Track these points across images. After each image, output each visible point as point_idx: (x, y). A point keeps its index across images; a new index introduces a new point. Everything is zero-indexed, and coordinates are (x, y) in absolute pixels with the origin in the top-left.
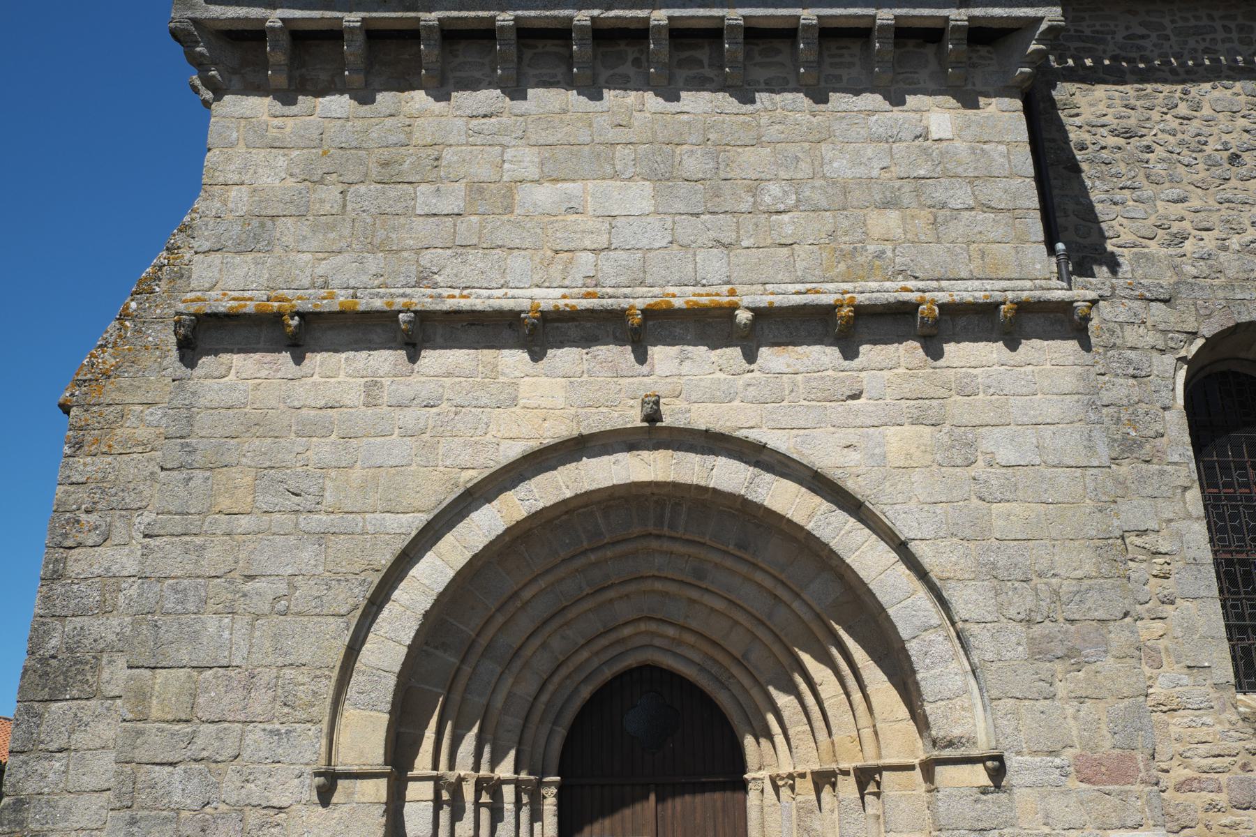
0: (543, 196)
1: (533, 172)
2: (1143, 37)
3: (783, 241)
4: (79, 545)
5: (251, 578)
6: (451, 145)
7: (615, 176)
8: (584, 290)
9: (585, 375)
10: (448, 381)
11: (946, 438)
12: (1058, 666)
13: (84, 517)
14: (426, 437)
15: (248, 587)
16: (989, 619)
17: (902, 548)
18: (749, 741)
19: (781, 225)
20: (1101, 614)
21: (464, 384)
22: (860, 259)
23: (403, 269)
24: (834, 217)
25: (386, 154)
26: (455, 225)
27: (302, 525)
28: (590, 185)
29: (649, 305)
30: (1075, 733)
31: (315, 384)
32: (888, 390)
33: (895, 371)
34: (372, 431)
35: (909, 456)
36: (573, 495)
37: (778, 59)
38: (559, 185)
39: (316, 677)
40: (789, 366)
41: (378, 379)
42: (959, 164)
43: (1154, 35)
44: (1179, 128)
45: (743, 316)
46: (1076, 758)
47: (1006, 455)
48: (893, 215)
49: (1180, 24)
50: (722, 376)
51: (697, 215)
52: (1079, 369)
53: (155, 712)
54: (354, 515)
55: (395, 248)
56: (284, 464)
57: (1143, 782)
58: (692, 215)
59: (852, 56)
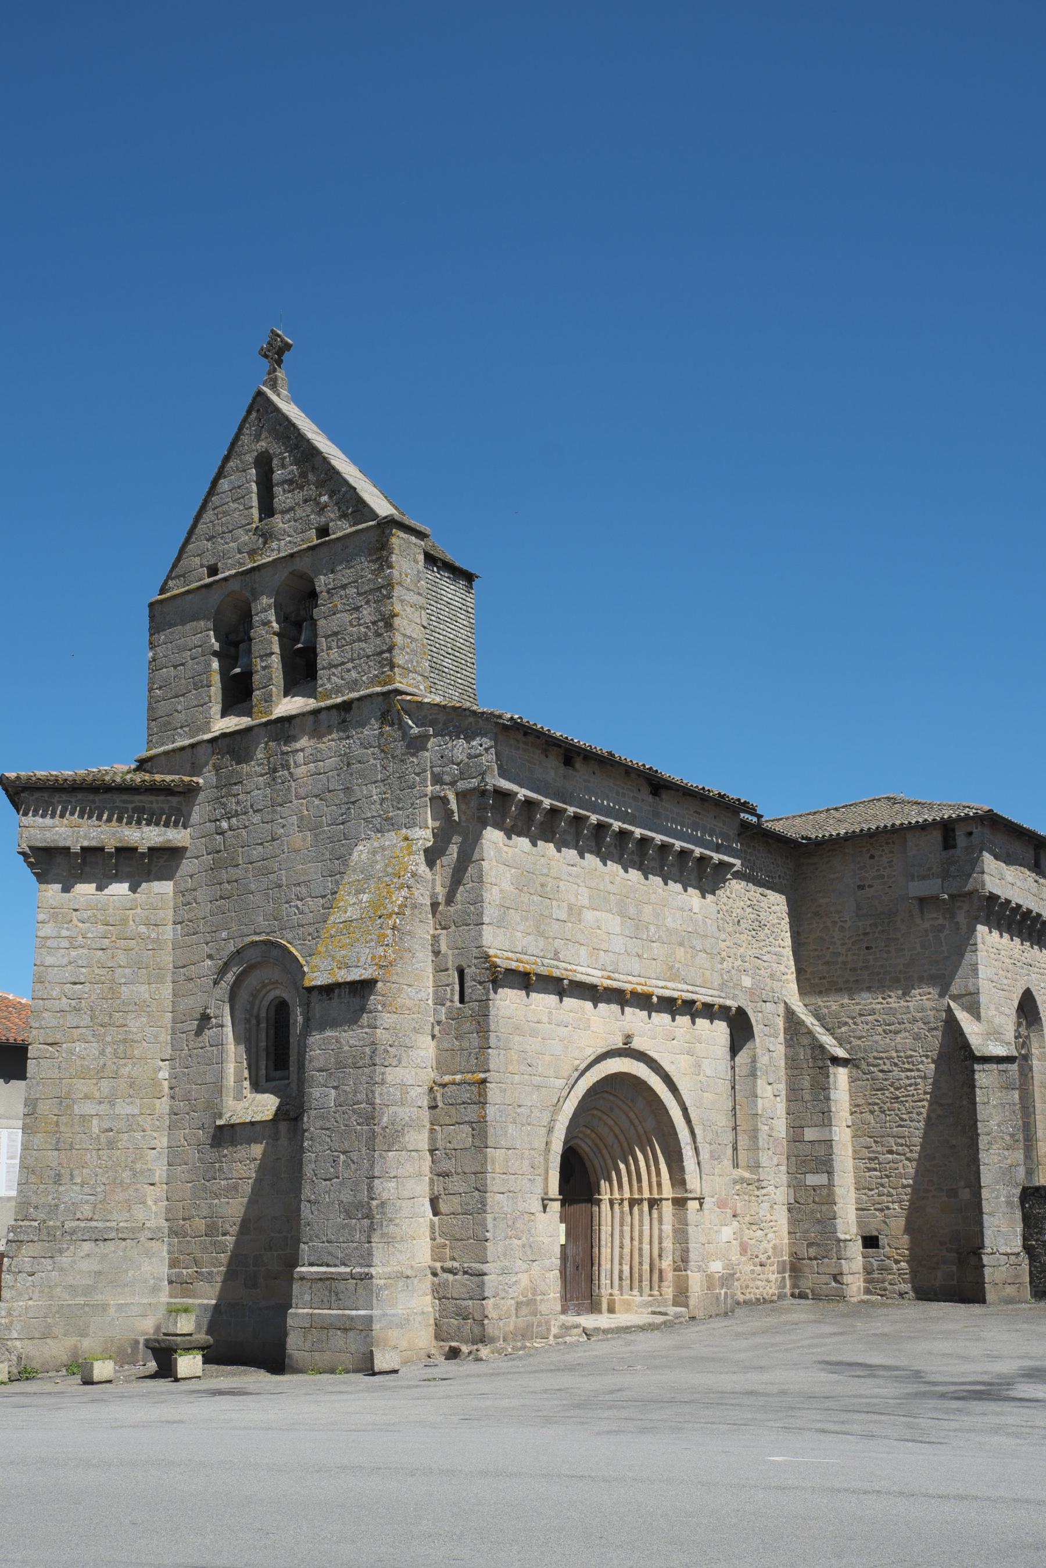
1: (586, 902)
5: (519, 1106)
8: (606, 974)
13: (389, 1048)
15: (519, 1110)
17: (685, 1110)
18: (602, 1182)
45: (655, 999)
48: (682, 949)
50: (642, 1024)
53: (498, 1170)
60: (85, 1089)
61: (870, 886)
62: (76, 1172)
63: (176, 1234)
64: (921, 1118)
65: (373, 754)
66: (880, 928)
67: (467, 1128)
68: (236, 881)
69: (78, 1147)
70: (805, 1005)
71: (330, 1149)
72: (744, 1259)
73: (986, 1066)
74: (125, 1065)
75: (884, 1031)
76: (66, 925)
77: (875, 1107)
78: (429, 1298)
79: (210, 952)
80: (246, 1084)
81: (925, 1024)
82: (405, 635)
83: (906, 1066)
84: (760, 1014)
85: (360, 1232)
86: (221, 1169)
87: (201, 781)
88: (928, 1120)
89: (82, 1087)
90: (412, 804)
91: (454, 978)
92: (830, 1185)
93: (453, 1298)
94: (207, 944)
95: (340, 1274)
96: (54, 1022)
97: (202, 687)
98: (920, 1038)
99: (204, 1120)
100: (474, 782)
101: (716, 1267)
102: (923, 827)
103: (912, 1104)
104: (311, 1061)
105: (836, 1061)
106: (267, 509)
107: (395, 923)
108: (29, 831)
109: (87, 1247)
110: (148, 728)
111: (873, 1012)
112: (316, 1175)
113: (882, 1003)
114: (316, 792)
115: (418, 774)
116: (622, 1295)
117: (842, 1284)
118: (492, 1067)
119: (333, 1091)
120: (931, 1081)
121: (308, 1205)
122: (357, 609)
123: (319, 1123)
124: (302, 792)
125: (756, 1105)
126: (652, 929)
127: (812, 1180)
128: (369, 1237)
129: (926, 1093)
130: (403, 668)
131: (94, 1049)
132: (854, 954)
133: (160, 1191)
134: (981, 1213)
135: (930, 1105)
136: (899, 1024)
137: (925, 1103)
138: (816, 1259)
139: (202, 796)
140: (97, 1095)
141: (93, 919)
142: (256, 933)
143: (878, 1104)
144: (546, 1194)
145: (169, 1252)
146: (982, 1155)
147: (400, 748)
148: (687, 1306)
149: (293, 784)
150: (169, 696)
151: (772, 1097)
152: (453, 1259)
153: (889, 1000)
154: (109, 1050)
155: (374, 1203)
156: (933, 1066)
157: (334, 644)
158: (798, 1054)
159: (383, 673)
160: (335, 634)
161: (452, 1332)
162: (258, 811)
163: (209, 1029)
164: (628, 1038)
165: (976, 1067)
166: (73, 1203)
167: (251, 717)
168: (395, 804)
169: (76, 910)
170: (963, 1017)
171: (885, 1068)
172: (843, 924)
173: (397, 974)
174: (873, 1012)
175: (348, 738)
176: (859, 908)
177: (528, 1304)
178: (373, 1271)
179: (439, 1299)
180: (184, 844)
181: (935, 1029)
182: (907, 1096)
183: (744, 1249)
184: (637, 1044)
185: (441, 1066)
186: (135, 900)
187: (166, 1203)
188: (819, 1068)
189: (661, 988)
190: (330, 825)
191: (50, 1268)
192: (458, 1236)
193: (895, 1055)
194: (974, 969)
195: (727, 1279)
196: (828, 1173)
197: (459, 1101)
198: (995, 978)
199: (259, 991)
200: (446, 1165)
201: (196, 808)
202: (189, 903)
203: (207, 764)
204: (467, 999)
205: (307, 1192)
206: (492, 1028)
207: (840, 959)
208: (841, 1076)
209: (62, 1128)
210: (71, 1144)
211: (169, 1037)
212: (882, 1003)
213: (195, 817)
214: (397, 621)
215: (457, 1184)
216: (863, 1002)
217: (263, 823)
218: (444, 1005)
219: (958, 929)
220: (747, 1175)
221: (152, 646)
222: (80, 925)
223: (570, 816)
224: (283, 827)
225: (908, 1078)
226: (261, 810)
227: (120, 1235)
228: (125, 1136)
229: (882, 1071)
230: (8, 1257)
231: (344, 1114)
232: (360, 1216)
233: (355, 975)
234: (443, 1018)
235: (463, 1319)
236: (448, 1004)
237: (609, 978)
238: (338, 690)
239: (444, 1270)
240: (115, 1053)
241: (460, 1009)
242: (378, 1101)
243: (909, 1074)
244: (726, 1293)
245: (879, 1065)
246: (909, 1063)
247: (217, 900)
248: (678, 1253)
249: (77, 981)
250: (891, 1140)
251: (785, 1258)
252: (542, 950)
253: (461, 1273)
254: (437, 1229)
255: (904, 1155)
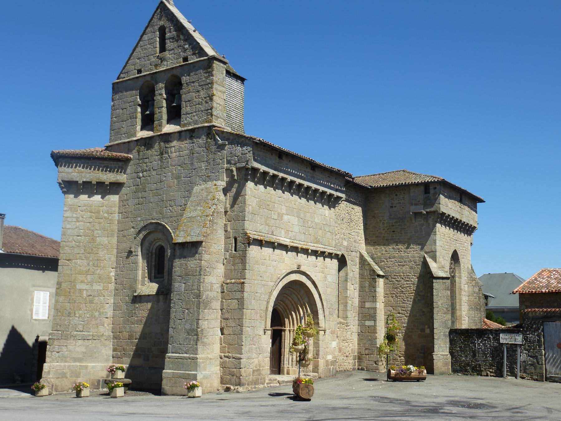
1: (284, 212)
4: (207, 275)
5: (257, 293)
8: (291, 241)
13: (206, 269)
17: (320, 295)
45: (310, 251)
48: (321, 231)
53: (247, 318)
60: (81, 279)
61: (395, 207)
62: (76, 312)
63: (116, 338)
64: (412, 300)
65: (203, 150)
66: (398, 224)
67: (236, 301)
68: (145, 198)
69: (77, 302)
70: (368, 253)
71: (182, 307)
72: (340, 354)
73: (438, 281)
74: (97, 270)
75: (398, 265)
76: (75, 213)
77: (394, 295)
78: (219, 367)
79: (133, 225)
80: (146, 279)
81: (415, 263)
82: (217, 103)
83: (407, 279)
85: (193, 341)
86: (135, 313)
87: (132, 156)
88: (414, 300)
89: (80, 278)
90: (218, 171)
91: (233, 241)
92: (375, 326)
93: (228, 368)
94: (132, 222)
95: (184, 357)
96: (69, 251)
97: (133, 118)
98: (413, 269)
99: (129, 293)
100: (244, 164)
101: (330, 357)
102: (417, 185)
103: (408, 294)
104: (175, 272)
105: (379, 276)
106: (163, 49)
107: (210, 219)
108: (62, 174)
109: (80, 342)
110: (110, 133)
111: (394, 257)
112: (175, 318)
113: (398, 254)
114: (179, 164)
115: (221, 160)
116: (292, 367)
117: (378, 365)
118: (246, 277)
119: (183, 285)
120: (416, 285)
121: (172, 329)
122: (198, 91)
123: (178, 297)
124: (173, 163)
125: (347, 293)
126: (310, 223)
127: (368, 323)
128: (197, 343)
129: (414, 290)
130: (216, 116)
131: (85, 262)
132: (388, 234)
133: (110, 321)
134: (433, 338)
135: (415, 295)
136: (405, 262)
137: (413, 294)
138: (368, 355)
139: (132, 162)
140: (86, 281)
141: (86, 210)
142: (152, 219)
143: (395, 294)
144: (266, 328)
145: (113, 345)
146: (435, 316)
147: (214, 148)
148: (318, 373)
149: (170, 160)
150: (120, 121)
151: (353, 290)
152: (229, 352)
153: (401, 252)
154: (91, 263)
155: (199, 330)
156: (417, 279)
157: (188, 105)
158: (364, 273)
159: (208, 118)
160: (189, 101)
161: (227, 381)
162: (155, 170)
163: (132, 256)
164: (299, 267)
165: (434, 281)
166: (75, 325)
167: (153, 132)
168: (211, 170)
169: (79, 206)
170: (429, 260)
171: (398, 280)
172: (383, 221)
173: (211, 239)
174: (394, 257)
175: (193, 143)
176: (390, 215)
177: (257, 371)
178: (197, 356)
179: (223, 368)
180: (124, 182)
181: (419, 265)
182: (406, 291)
183: (340, 350)
184: (302, 269)
185: (226, 276)
186: (103, 203)
187: (112, 325)
188: (373, 279)
189: (312, 247)
190: (184, 178)
191: (65, 350)
192: (231, 343)
193: (402, 274)
194: (435, 242)
195: (334, 362)
196: (374, 321)
197: (233, 290)
198: (443, 246)
199: (152, 242)
200: (227, 316)
201: (129, 167)
202: (125, 205)
203: (134, 149)
204: (237, 250)
205: (171, 324)
206: (247, 261)
207: (382, 235)
208: (381, 282)
209: (72, 294)
210: (75, 301)
211: (115, 259)
212: (398, 254)
213: (128, 171)
214: (214, 98)
215: (232, 323)
216: (391, 253)
217: (157, 175)
218: (228, 252)
219: (429, 226)
220: (342, 321)
221: (113, 100)
222: (81, 212)
223: (280, 178)
224: (165, 177)
225: (407, 284)
226: (156, 170)
227: (94, 338)
228: (97, 298)
229: (397, 281)
230: (49, 345)
231: (188, 294)
232: (193, 334)
233: (195, 239)
234: (228, 257)
235: (232, 376)
236: (230, 251)
237: (293, 242)
238: (189, 124)
239: (225, 356)
240: (94, 264)
241: (234, 254)
242: (202, 289)
243: (407, 282)
244: (333, 368)
245: (396, 278)
246: (407, 278)
247: (137, 205)
248: (315, 352)
249: (79, 235)
250: (400, 308)
251: (356, 354)
252: (267, 231)
253: (232, 358)
254: (223, 340)
255: (404, 314)
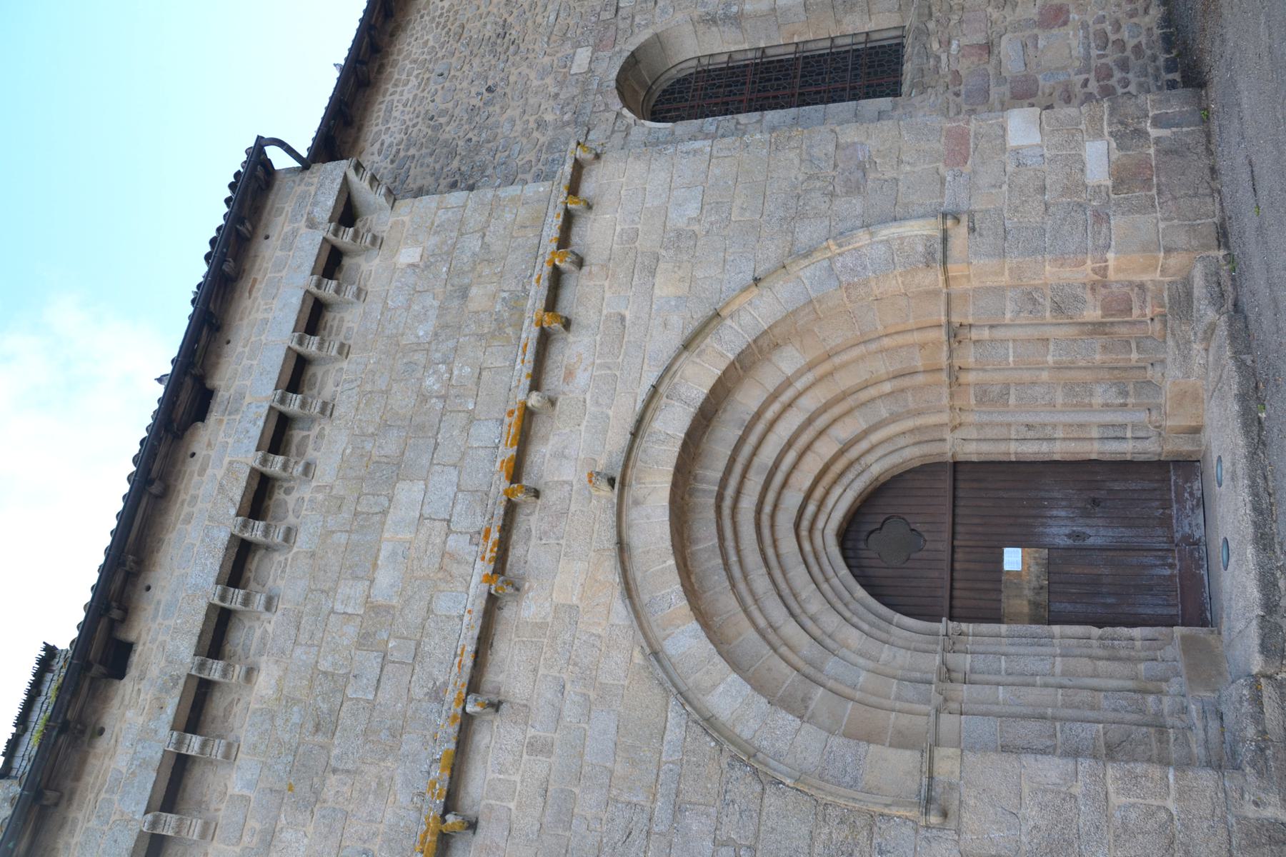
0: (386, 578)
1: (362, 586)
2: (382, 144)
3: (476, 375)
6: (317, 662)
7: (384, 513)
9: (561, 542)
10: (542, 671)
11: (672, 252)
12: (872, 176)
14: (593, 695)
16: (827, 223)
19: (460, 376)
20: (831, 148)
21: (548, 655)
22: (506, 315)
23: (424, 715)
24: (465, 336)
25: (310, 726)
26: (393, 662)
27: (662, 828)
28: (386, 535)
29: (507, 477)
30: (926, 166)
31: (519, 806)
32: (622, 294)
33: (606, 289)
34: (578, 749)
35: (682, 280)
36: (673, 557)
37: (319, 375)
38: (379, 562)
39: (824, 820)
40: (586, 370)
41: (527, 741)
42: (444, 243)
43: (383, 137)
44: (457, 122)
46: (946, 165)
47: (692, 210)
48: (474, 291)
49: (380, 121)
50: (585, 423)
51: (437, 444)
52: (631, 159)
54: (661, 774)
55: (401, 723)
56: (596, 845)
57: (968, 124)
58: (435, 449)
59: (334, 319)
84: (637, 19)
244: (1157, 122)
